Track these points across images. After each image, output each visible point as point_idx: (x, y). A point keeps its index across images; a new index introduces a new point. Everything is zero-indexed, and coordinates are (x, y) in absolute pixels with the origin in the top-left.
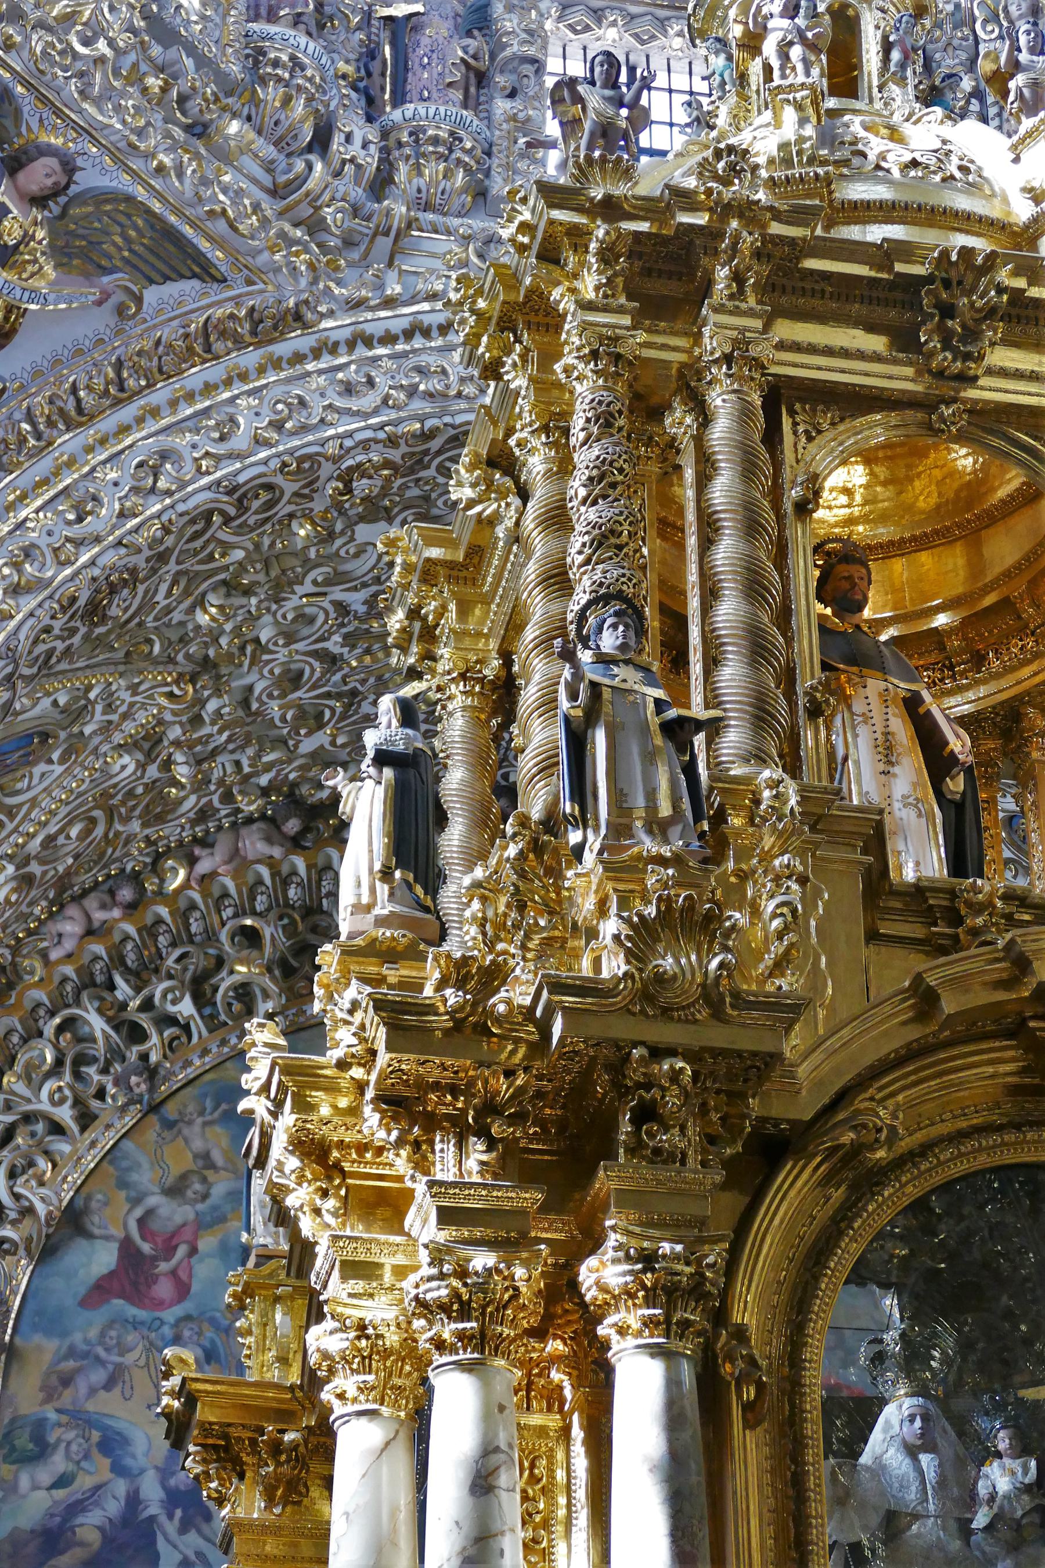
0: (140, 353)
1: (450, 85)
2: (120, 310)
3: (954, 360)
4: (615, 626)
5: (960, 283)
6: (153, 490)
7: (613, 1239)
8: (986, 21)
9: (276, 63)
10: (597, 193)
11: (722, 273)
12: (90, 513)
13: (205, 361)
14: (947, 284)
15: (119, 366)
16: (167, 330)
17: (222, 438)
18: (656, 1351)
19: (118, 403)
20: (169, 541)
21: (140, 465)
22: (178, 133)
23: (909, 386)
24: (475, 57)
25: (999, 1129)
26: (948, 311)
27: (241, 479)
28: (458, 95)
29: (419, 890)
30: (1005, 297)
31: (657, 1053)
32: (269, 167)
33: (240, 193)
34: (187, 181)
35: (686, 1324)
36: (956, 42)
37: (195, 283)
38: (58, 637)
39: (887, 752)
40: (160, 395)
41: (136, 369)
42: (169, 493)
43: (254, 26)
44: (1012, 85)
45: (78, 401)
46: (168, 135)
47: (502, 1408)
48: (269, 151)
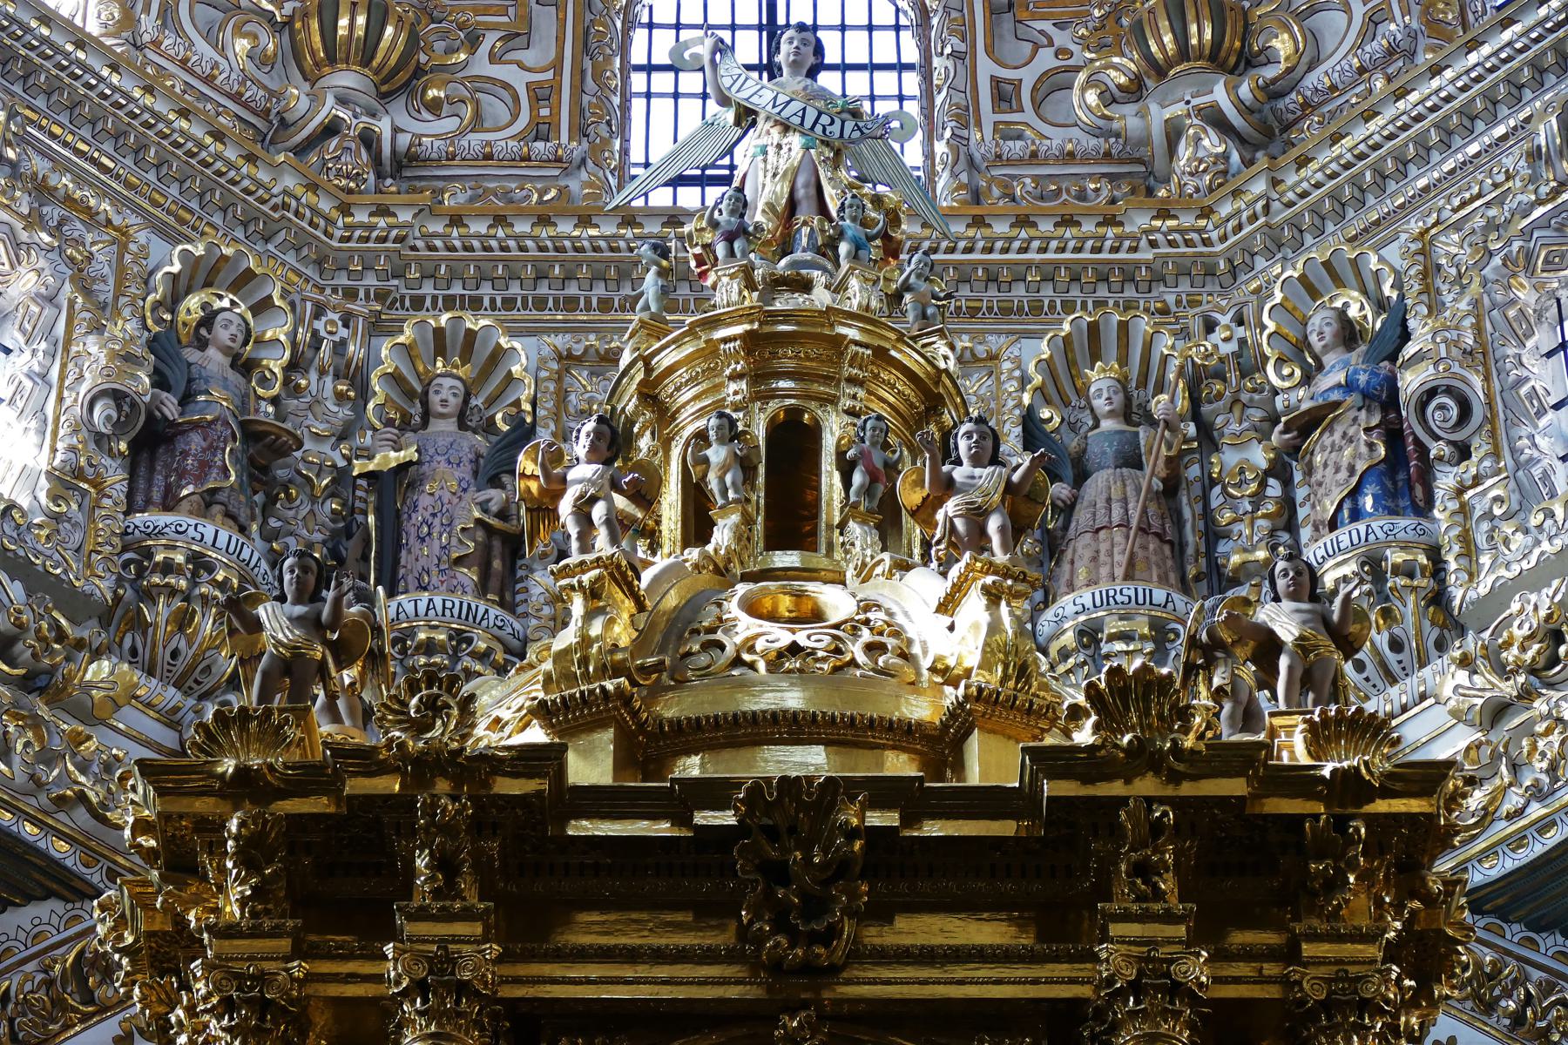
1: (459, 561)
3: (792, 946)
5: (792, 830)
8: (1280, 361)
9: (168, 568)
10: (228, 766)
13: (85, 1018)
14: (772, 834)
16: (17, 979)
23: (733, 992)
24: (503, 515)
26: (778, 873)
28: (469, 575)
30: (857, 845)
34: (17, 760)
36: (1245, 397)
37: (56, 905)
43: (139, 518)
44: (940, 516)
48: (172, 696)
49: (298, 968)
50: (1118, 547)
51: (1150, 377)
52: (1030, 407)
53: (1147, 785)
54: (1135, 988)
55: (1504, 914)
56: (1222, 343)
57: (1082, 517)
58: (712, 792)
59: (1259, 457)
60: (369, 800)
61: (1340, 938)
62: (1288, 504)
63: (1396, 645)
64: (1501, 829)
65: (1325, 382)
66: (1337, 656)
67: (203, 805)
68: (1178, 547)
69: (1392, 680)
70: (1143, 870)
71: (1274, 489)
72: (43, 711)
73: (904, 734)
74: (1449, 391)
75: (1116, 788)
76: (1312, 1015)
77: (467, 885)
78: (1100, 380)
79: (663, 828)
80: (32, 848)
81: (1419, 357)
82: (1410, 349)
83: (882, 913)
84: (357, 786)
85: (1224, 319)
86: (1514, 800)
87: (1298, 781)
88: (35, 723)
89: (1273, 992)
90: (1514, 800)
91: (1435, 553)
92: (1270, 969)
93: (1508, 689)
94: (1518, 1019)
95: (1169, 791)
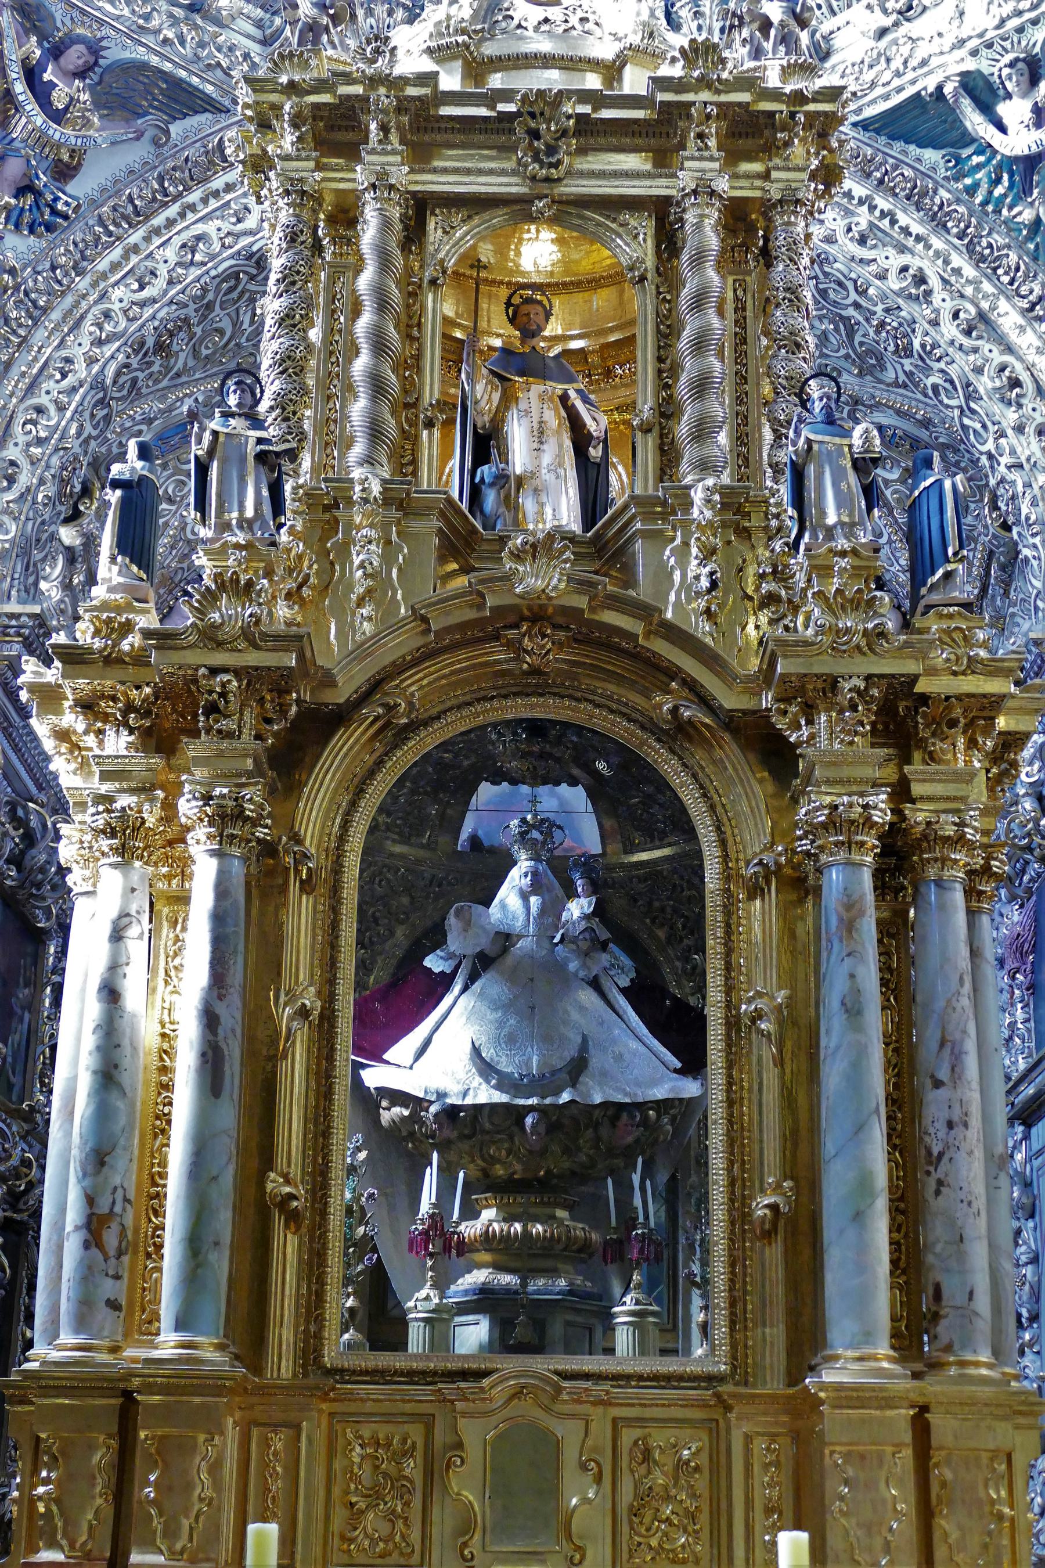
0: (174, 169)
2: (156, 143)
3: (541, 168)
4: (235, 392)
5: (542, 114)
6: (192, 263)
7: (187, 788)
10: (284, 79)
11: (373, 126)
12: (149, 283)
13: (224, 169)
14: (533, 115)
15: (161, 179)
16: (192, 150)
17: (239, 221)
18: (213, 853)
19: (165, 205)
20: (210, 296)
21: (184, 246)
22: (179, 12)
23: (514, 190)
25: (469, 704)
26: (535, 134)
27: (255, 248)
29: (135, 569)
30: (572, 122)
31: (214, 671)
32: (259, 24)
33: (231, 49)
35: (233, 836)
37: (208, 115)
38: (137, 370)
39: (540, 434)
40: (194, 197)
41: (173, 181)
42: (204, 264)
45: (135, 207)
46: (171, 15)
47: (133, 890)
48: (259, 13)
49: (318, 176)
53: (705, 96)
54: (695, 192)
55: (878, 132)
58: (506, 95)
60: (349, 97)
61: (789, 169)
64: (879, 91)
66: (798, 30)
67: (274, 98)
69: (833, 13)
70: (701, 136)
72: (199, 22)
73: (594, 64)
75: (689, 97)
76: (774, 206)
77: (394, 137)
79: (483, 112)
80: (196, 89)
83: (582, 151)
84: (344, 90)
87: (775, 95)
88: (196, 27)
89: (757, 194)
90: (887, 76)
92: (758, 183)
93: (888, 22)
94: (881, 182)
95: (716, 98)
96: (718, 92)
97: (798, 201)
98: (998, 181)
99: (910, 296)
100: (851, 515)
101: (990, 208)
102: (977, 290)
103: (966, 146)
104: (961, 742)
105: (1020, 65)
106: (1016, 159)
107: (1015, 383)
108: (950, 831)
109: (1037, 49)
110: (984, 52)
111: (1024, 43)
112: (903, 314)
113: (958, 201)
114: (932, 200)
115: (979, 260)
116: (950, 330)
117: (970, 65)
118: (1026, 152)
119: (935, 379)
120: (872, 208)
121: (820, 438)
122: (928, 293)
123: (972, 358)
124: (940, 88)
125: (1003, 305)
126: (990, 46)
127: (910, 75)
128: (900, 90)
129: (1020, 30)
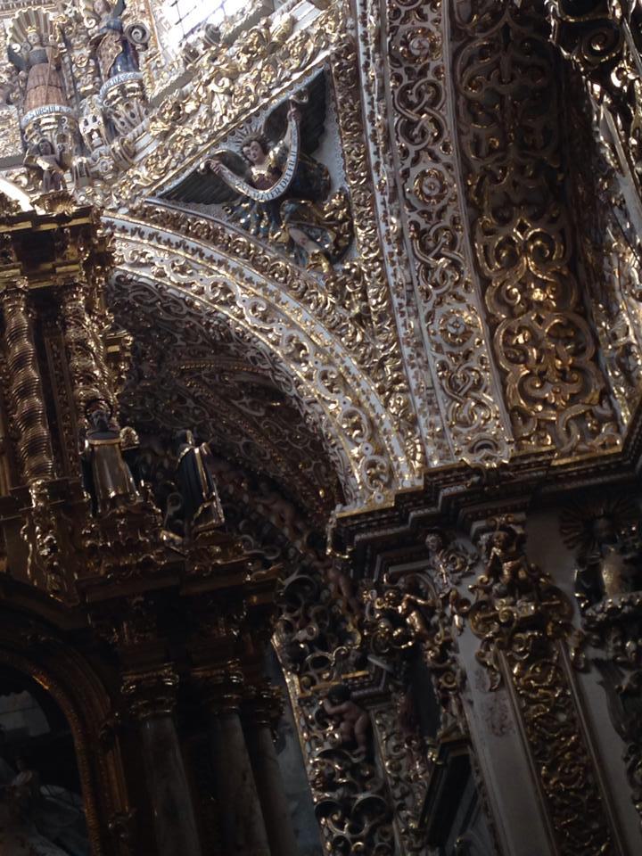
8: (88, 18)
36: (79, 31)
50: (42, 91)
51: (49, 26)
52: (10, 46)
55: (177, 199)
56: (70, 12)
57: (30, 82)
59: (86, 52)
61: (67, 264)
62: (97, 67)
63: (133, 115)
64: (171, 174)
65: (104, 24)
66: (61, 172)
68: (62, 88)
69: (133, 127)
71: (92, 63)
74: (138, 27)
78: (31, 32)
81: (127, 16)
82: (125, 13)
85: (69, 5)
86: (173, 164)
87: (45, 219)
90: (173, 164)
91: (141, 82)
95: (11, 229)
96: (10, 225)
97: (76, 285)
98: (261, 217)
99: (222, 303)
100: (125, 489)
101: (261, 235)
102: (265, 290)
103: (234, 200)
104: (221, 620)
105: (253, 143)
106: (267, 203)
107: (301, 347)
108: (220, 680)
109: (262, 133)
110: (230, 138)
111: (253, 129)
112: (219, 315)
113: (240, 235)
114: (222, 236)
115: (262, 270)
116: (250, 320)
117: (223, 148)
118: (271, 198)
119: (249, 355)
120: (186, 249)
121: (96, 442)
122: (233, 298)
123: (270, 336)
124: (208, 165)
125: (284, 297)
126: (232, 133)
127: (188, 160)
128: (183, 170)
129: (249, 121)
